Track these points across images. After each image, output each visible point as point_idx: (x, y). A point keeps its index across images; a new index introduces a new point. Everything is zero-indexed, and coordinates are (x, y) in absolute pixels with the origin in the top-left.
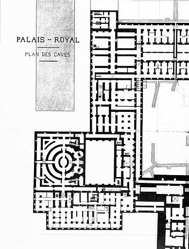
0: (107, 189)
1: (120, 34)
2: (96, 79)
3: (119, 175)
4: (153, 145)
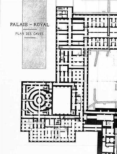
0: (66, 117)
1: (74, 21)
2: (59, 49)
3: (73, 108)
4: (95, 89)
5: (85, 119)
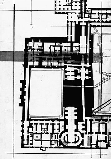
5: (81, 24)
